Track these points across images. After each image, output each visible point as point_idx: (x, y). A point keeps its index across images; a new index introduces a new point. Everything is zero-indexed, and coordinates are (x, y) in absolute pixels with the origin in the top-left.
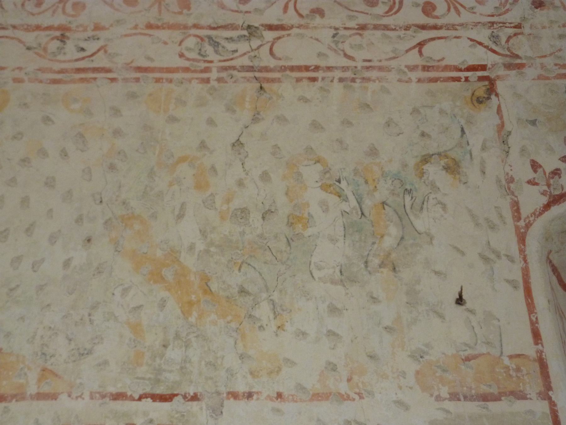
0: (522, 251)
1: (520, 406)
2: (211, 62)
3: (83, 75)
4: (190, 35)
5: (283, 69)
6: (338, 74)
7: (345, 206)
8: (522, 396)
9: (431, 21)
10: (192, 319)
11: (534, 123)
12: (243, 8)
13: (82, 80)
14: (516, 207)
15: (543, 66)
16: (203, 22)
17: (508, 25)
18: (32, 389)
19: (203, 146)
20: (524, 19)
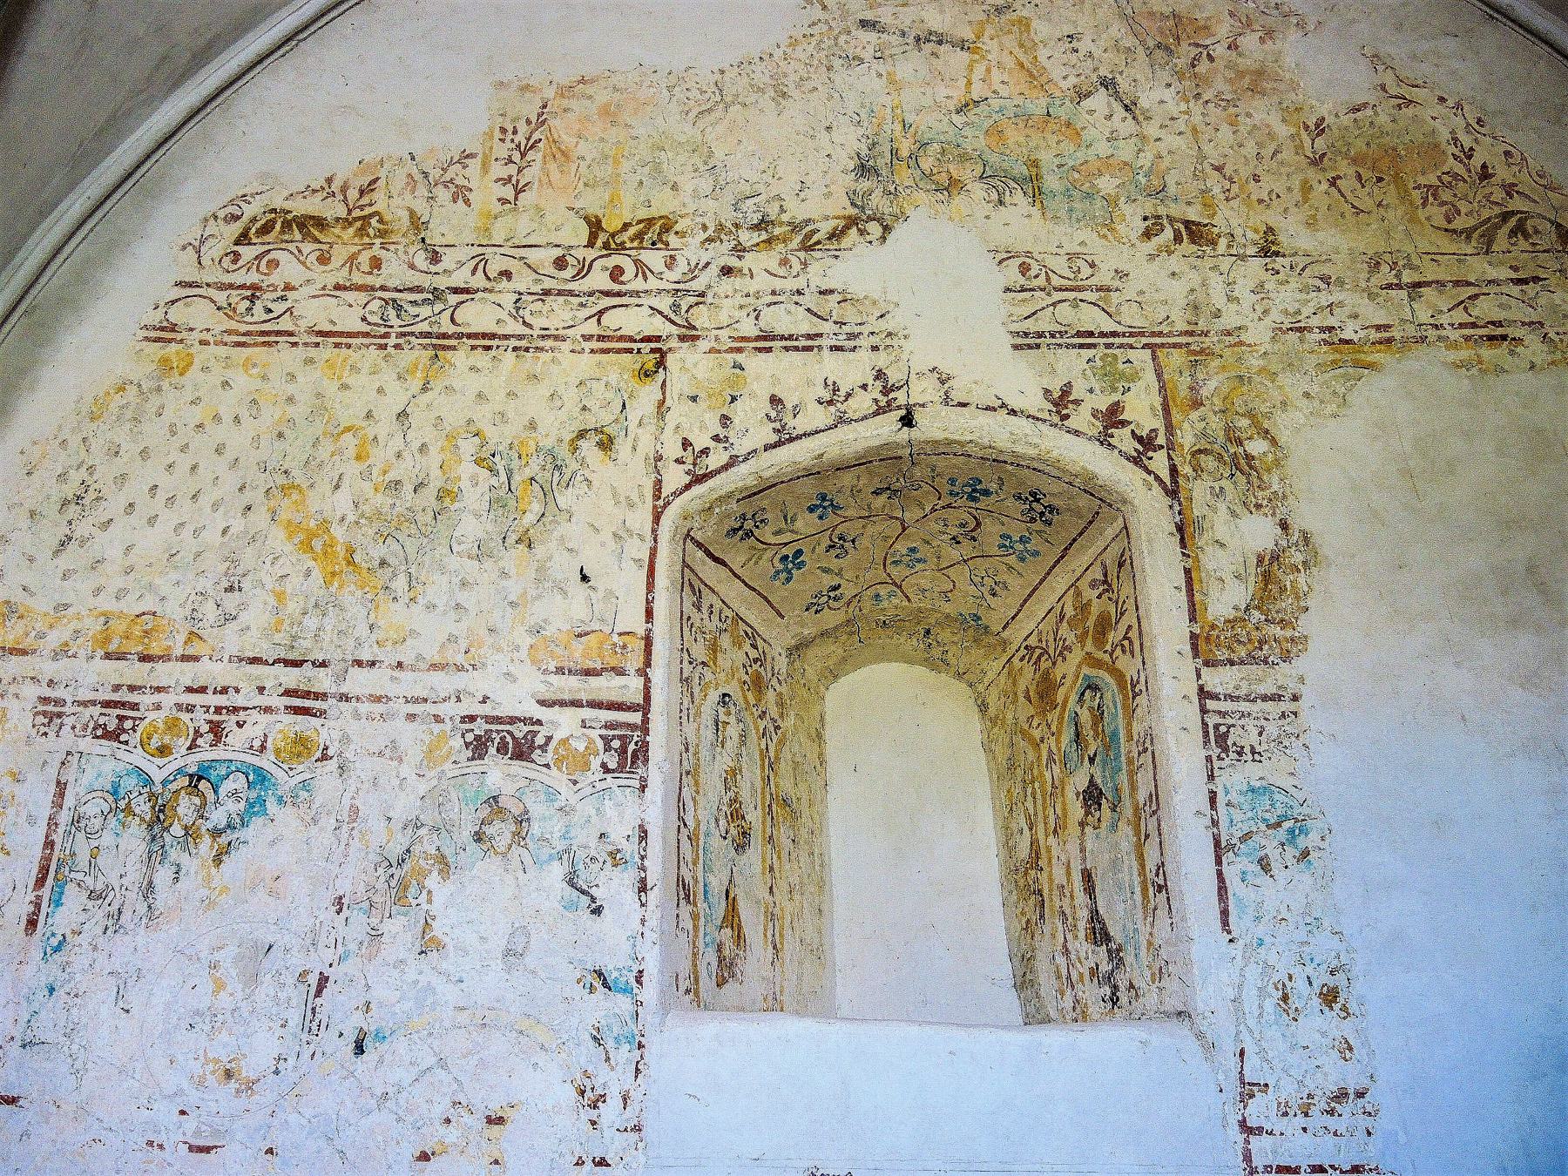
0: (654, 531)
1: (620, 680)
2: (392, 327)
3: (267, 339)
4: (375, 298)
5: (460, 336)
6: (513, 343)
7: (494, 481)
8: (621, 672)
9: (616, 287)
10: (333, 589)
11: (694, 399)
12: (433, 269)
13: (264, 344)
14: (658, 484)
15: (717, 339)
16: (391, 284)
17: (691, 293)
18: (178, 652)
19: (369, 415)
20: (710, 287)
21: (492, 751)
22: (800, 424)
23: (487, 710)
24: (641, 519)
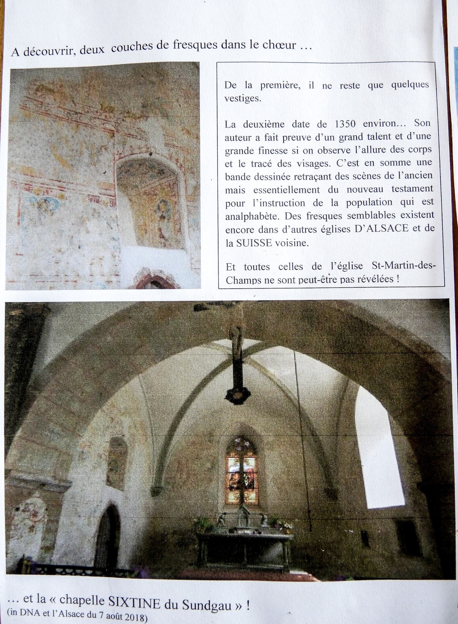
21: (93, 201)
22: (135, 152)
23: (91, 194)
24: (112, 164)
